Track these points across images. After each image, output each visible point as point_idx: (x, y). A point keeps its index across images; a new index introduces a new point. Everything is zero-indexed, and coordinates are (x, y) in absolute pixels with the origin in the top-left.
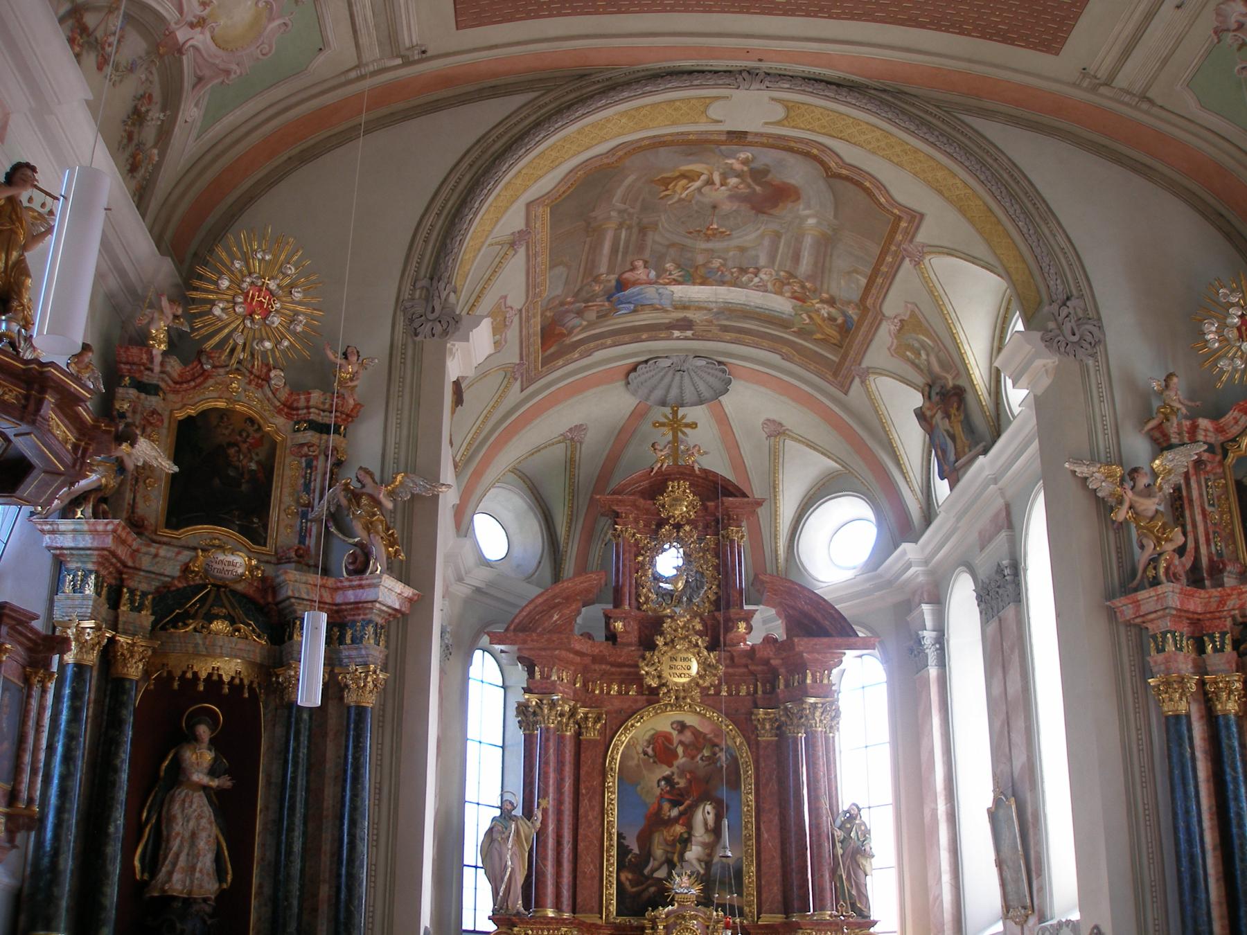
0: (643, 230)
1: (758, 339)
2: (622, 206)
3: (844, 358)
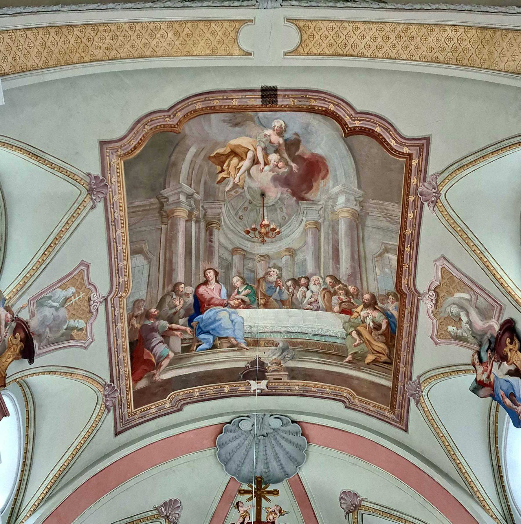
2: (190, 190)
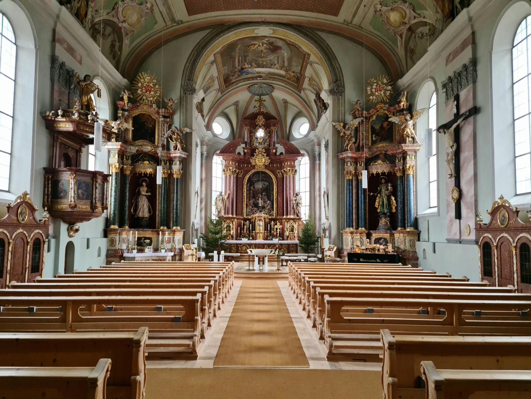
0: (245, 57)
1: (279, 80)
3: (299, 85)
